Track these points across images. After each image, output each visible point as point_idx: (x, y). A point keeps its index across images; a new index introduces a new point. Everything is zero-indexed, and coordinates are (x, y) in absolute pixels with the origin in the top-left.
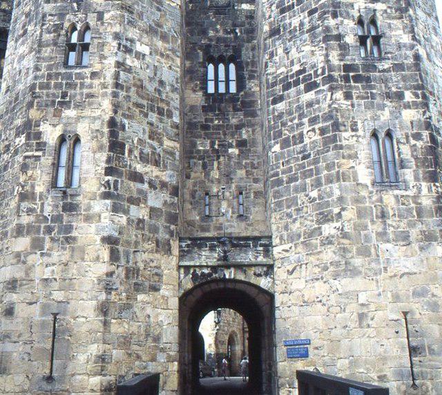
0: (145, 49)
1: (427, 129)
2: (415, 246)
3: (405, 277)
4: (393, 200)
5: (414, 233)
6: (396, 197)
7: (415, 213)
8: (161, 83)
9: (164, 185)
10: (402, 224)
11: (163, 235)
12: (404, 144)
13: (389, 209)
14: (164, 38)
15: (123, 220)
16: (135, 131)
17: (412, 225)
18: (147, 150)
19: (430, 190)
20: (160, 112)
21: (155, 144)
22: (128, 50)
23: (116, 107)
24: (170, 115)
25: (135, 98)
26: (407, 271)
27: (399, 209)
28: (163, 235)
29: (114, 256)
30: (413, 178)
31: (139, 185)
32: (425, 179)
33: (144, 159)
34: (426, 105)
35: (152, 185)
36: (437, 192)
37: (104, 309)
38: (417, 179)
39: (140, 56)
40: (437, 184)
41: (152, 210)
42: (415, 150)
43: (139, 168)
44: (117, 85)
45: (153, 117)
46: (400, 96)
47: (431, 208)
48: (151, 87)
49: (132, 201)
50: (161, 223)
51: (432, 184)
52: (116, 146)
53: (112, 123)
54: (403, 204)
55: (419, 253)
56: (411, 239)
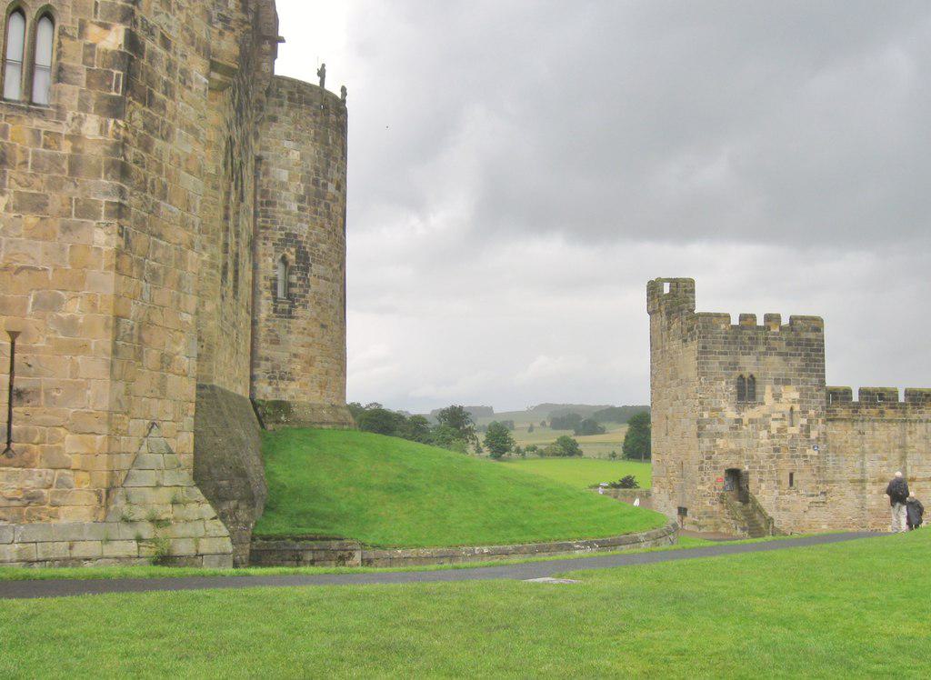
1: (123, 20)
2: (56, 224)
3: (25, 272)
4: (28, 136)
5: (56, 201)
6: (36, 133)
7: (65, 166)
10: (37, 182)
12: (72, 38)
13: (18, 153)
17: (55, 185)
19: (103, 129)
26: (30, 263)
27: (36, 154)
30: (75, 103)
32: (98, 108)
36: (117, 136)
38: (83, 107)
40: (120, 122)
42: (92, 55)
47: (98, 161)
51: (112, 121)
54: (46, 146)
55: (59, 234)
56: (49, 208)
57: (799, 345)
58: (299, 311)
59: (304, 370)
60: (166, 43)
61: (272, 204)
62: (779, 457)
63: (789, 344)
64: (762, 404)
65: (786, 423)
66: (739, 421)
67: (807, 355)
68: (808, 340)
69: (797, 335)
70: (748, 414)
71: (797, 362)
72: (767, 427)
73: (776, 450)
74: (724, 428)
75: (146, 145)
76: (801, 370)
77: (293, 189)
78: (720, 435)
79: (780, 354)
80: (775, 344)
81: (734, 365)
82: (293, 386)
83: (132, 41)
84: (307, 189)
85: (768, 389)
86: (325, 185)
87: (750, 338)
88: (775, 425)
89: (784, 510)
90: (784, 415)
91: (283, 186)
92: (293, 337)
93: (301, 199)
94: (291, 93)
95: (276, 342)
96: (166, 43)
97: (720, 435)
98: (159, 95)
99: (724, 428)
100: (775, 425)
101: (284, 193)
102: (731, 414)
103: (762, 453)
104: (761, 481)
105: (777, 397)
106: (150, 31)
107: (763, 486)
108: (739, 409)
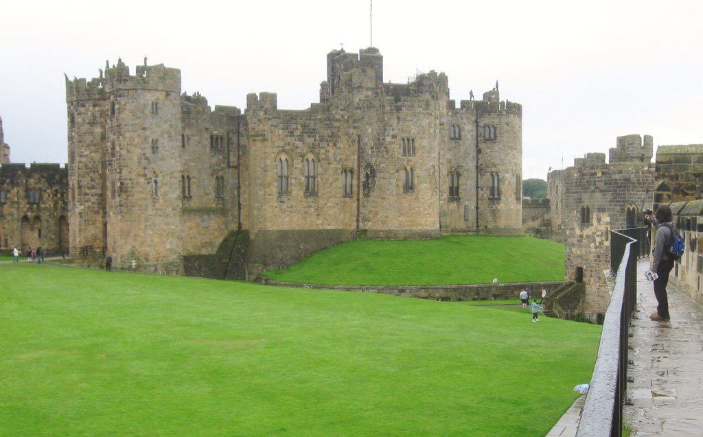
0: (87, 153)
8: (94, 162)
9: (96, 194)
11: (96, 209)
14: (94, 145)
15: (82, 207)
16: (85, 181)
18: (90, 186)
20: (94, 172)
21: (93, 183)
22: (81, 156)
23: (79, 175)
24: (97, 172)
25: (84, 170)
28: (96, 209)
29: (81, 217)
31: (87, 197)
33: (89, 188)
34: (120, 172)
35: (92, 195)
37: (80, 230)
39: (86, 156)
41: (93, 203)
43: (88, 191)
44: (79, 169)
45: (92, 175)
46: (116, 170)
48: (90, 165)
49: (85, 201)
50: (96, 206)
52: (80, 187)
53: (78, 181)
57: (611, 184)
58: (371, 194)
59: (374, 217)
60: (130, 180)
61: (363, 152)
62: (600, 261)
63: (606, 184)
64: (592, 225)
65: (604, 238)
66: (581, 236)
67: (615, 191)
68: (616, 180)
69: (610, 177)
70: (587, 232)
71: (609, 196)
72: (594, 241)
73: (598, 256)
74: (575, 241)
75: (127, 199)
76: (610, 201)
77: (369, 144)
78: (573, 245)
79: (601, 191)
80: (598, 184)
81: (580, 200)
82: (370, 223)
83: (122, 184)
84: (375, 144)
85: (595, 214)
86: (384, 139)
87: (587, 182)
88: (598, 239)
89: (602, 297)
90: (602, 233)
91: (366, 144)
92: (369, 204)
93: (372, 148)
94: (367, 105)
95: (364, 207)
96: (130, 180)
97: (573, 245)
98: (129, 189)
99: (575, 241)
100: (598, 239)
101: (367, 147)
102: (578, 232)
103: (592, 258)
104: (591, 276)
105: (599, 220)
106: (126, 179)
107: (592, 279)
108: (582, 229)
